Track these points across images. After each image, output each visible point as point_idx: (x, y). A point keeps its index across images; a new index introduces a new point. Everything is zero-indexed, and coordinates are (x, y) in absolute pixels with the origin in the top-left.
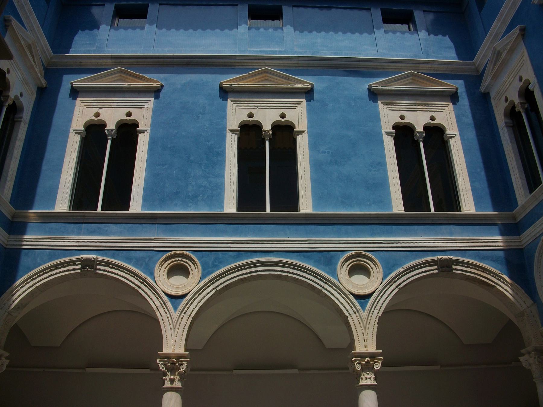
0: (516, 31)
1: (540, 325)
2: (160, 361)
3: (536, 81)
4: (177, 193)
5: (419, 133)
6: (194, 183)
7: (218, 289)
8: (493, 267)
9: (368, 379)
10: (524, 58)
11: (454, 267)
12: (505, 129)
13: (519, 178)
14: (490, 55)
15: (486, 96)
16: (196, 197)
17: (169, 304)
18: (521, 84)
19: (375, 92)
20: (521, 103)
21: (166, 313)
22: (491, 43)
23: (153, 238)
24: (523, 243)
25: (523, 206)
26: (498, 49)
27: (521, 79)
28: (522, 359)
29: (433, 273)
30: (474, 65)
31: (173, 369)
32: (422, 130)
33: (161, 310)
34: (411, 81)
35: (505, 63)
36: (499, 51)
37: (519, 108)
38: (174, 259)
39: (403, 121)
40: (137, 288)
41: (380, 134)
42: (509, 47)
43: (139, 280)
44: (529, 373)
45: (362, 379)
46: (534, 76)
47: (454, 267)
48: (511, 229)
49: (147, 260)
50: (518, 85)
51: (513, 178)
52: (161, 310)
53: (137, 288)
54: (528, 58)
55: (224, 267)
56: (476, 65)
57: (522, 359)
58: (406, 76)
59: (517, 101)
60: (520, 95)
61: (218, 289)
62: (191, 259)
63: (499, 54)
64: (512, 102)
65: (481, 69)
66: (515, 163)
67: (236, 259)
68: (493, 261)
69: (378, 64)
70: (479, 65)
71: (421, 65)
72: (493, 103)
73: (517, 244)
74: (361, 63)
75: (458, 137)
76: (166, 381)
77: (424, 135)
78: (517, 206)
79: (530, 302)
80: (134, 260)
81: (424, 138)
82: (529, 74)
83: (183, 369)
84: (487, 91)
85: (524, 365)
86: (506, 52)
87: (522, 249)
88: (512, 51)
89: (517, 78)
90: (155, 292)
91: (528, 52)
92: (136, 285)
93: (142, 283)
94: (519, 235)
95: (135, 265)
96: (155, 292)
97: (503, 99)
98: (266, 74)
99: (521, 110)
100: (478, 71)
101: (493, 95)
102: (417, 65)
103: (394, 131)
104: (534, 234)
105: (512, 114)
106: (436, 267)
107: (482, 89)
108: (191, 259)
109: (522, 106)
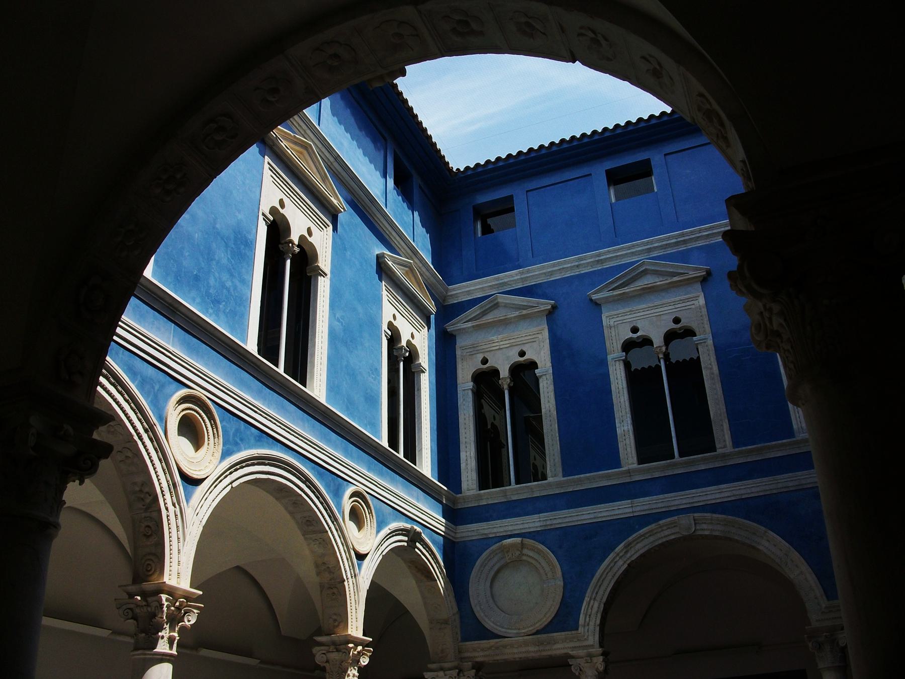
2: (167, 600)
4: (197, 278)
6: (217, 275)
7: (235, 485)
11: (418, 544)
16: (219, 302)
17: (181, 489)
21: (174, 505)
23: (171, 348)
26: (499, 300)
27: (522, 354)
31: (174, 620)
33: (168, 496)
36: (498, 303)
40: (136, 438)
43: (142, 424)
45: (349, 676)
47: (418, 544)
48: (452, 514)
49: (157, 387)
51: (463, 455)
52: (168, 496)
53: (136, 438)
55: (245, 449)
61: (235, 485)
62: (211, 417)
67: (258, 442)
69: (390, 229)
70: (451, 295)
72: (458, 353)
75: (427, 374)
76: (160, 641)
80: (139, 378)
83: (191, 620)
87: (454, 542)
90: (164, 458)
92: (136, 430)
93: (146, 431)
94: (456, 525)
95: (141, 388)
96: (164, 458)
98: (305, 152)
99: (506, 387)
104: (486, 532)
106: (406, 539)
108: (211, 417)
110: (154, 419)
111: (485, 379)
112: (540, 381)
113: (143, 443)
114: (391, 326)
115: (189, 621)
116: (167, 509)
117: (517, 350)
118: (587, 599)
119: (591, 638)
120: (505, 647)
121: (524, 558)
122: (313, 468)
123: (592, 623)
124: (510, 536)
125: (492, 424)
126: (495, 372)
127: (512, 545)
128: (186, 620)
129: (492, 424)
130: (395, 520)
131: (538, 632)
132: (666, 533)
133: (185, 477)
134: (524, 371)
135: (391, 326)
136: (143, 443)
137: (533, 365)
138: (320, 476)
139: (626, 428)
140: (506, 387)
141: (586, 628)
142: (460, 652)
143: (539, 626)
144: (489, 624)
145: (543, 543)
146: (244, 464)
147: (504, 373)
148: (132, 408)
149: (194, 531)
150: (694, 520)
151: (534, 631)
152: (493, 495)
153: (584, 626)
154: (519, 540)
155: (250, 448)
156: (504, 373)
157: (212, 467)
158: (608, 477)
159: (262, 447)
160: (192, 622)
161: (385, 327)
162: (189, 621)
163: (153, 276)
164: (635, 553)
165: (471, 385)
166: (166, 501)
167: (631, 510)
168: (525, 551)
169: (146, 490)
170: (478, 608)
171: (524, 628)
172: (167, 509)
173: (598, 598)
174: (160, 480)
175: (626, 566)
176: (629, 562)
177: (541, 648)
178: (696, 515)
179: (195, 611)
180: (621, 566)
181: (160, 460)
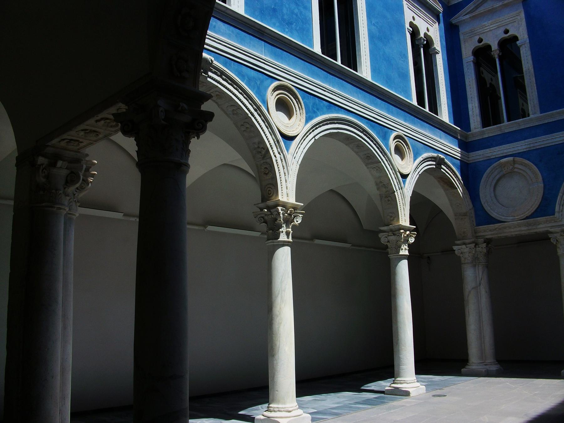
4: (274, 10)
6: (287, 6)
7: (316, 138)
9: (404, 251)
11: (442, 166)
17: (282, 143)
21: (279, 153)
23: (264, 57)
27: (506, 32)
31: (288, 222)
33: (275, 148)
38: (286, 93)
40: (250, 115)
41: (404, 26)
43: (252, 106)
45: (402, 249)
47: (442, 166)
48: (465, 145)
49: (258, 83)
51: (470, 106)
52: (275, 148)
53: (250, 115)
55: (321, 115)
61: (316, 138)
62: (296, 97)
67: (329, 110)
72: (462, 37)
75: (440, 54)
76: (281, 234)
83: (298, 221)
87: (468, 164)
90: (269, 126)
92: (249, 111)
93: (256, 110)
95: (248, 84)
96: (269, 126)
99: (496, 56)
106: (434, 163)
108: (296, 97)
110: (259, 103)
111: (482, 53)
112: (521, 48)
113: (255, 118)
114: (411, 24)
115: (297, 221)
116: (275, 156)
117: (503, 29)
118: (560, 194)
120: (505, 228)
121: (516, 170)
122: (367, 123)
124: (505, 157)
125: (491, 84)
126: (488, 47)
127: (507, 162)
128: (295, 221)
129: (491, 84)
130: (426, 152)
131: (527, 218)
133: (283, 136)
134: (509, 44)
135: (411, 24)
136: (255, 118)
137: (515, 38)
138: (372, 128)
140: (496, 56)
141: (561, 213)
142: (476, 233)
143: (528, 213)
144: (494, 214)
145: (528, 160)
146: (321, 125)
147: (495, 46)
148: (244, 97)
149: (294, 168)
151: (525, 217)
152: (492, 131)
153: (559, 212)
154: (511, 158)
155: (324, 114)
156: (495, 46)
157: (300, 128)
159: (332, 113)
160: (299, 222)
161: (407, 26)
162: (297, 221)
163: (245, 13)
165: (472, 58)
166: (274, 151)
168: (516, 166)
169: (261, 146)
170: (486, 204)
171: (517, 216)
172: (275, 156)
174: (268, 139)
177: (530, 228)
179: (301, 215)
181: (267, 127)
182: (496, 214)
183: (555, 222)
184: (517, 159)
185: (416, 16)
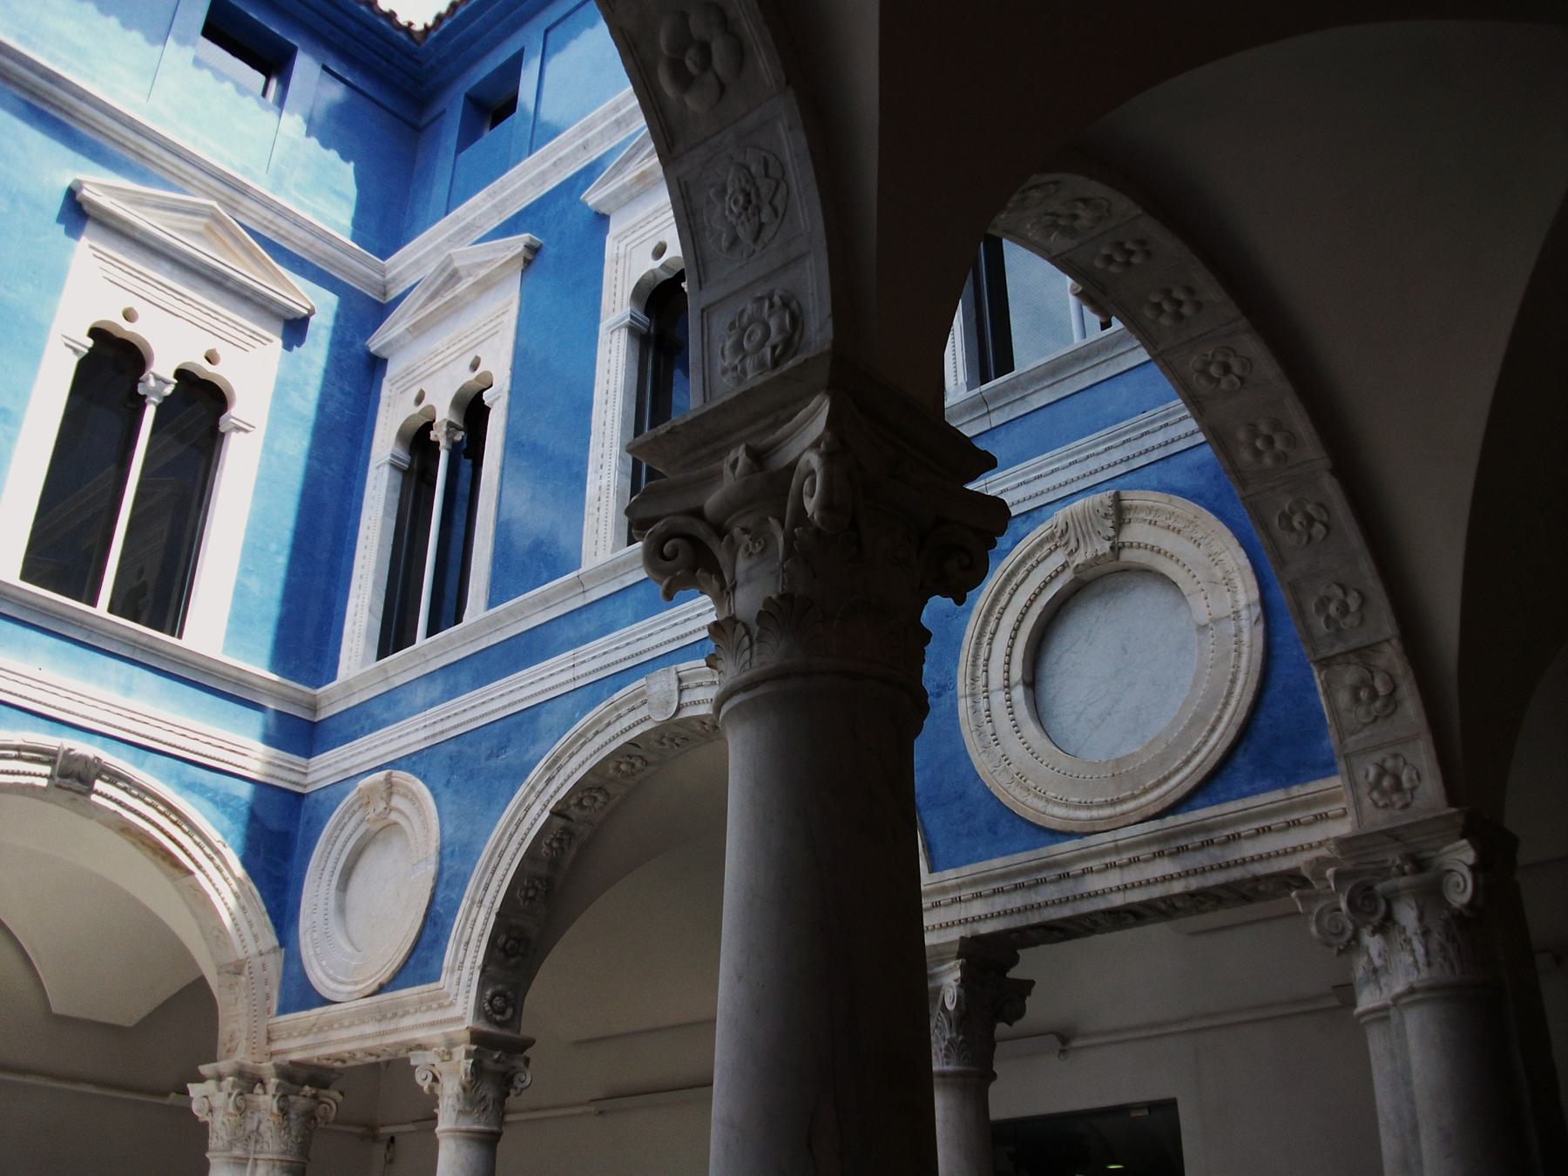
0: (517, 243)
1: (275, 1008)
3: (507, 387)
5: (157, 378)
8: (207, 817)
10: (505, 318)
12: (386, 470)
13: (366, 610)
14: (431, 268)
15: (376, 365)
18: (472, 376)
19: (86, 208)
20: (450, 424)
22: (448, 240)
24: (310, 779)
25: (348, 685)
26: (457, 264)
27: (474, 366)
28: (195, 1090)
29: (33, 786)
30: (383, 272)
32: (170, 376)
34: (200, 228)
35: (455, 308)
37: (438, 434)
39: (127, 326)
41: (38, 331)
42: (483, 273)
44: (199, 1132)
46: (508, 372)
50: (463, 377)
54: (513, 323)
56: (389, 276)
57: (195, 1090)
58: (194, 211)
59: (444, 413)
60: (457, 403)
63: (454, 277)
64: (431, 410)
65: (394, 293)
66: (372, 566)
68: (215, 803)
69: (131, 135)
70: (394, 279)
71: (248, 203)
73: (294, 777)
74: (84, 107)
77: (169, 390)
78: (333, 677)
79: (271, 940)
81: (166, 398)
82: (499, 365)
84: (384, 354)
85: (195, 1107)
86: (471, 280)
87: (302, 795)
88: (485, 286)
89: (469, 359)
91: (520, 309)
94: (309, 754)
97: (414, 393)
99: (443, 443)
100: (385, 294)
101: (392, 370)
102: (238, 197)
103: (90, 343)
104: (346, 765)
105: (418, 440)
106: (47, 770)
107: (375, 344)
109: (448, 432)
118: (465, 903)
119: (461, 999)
120: (331, 1024)
121: (394, 816)
123: (468, 964)
127: (372, 788)
131: (382, 989)
132: (626, 722)
139: (604, 482)
141: (457, 974)
142: (270, 1040)
143: (384, 976)
145: (424, 779)
150: (680, 680)
151: (375, 987)
153: (453, 971)
154: (380, 776)
158: (545, 601)
164: (562, 785)
167: (569, 675)
173: (487, 902)
175: (546, 814)
176: (551, 806)
177: (384, 1026)
178: (682, 667)
180: (538, 816)
182: (320, 973)
183: (441, 1006)
184: (401, 776)
185: (139, 306)
